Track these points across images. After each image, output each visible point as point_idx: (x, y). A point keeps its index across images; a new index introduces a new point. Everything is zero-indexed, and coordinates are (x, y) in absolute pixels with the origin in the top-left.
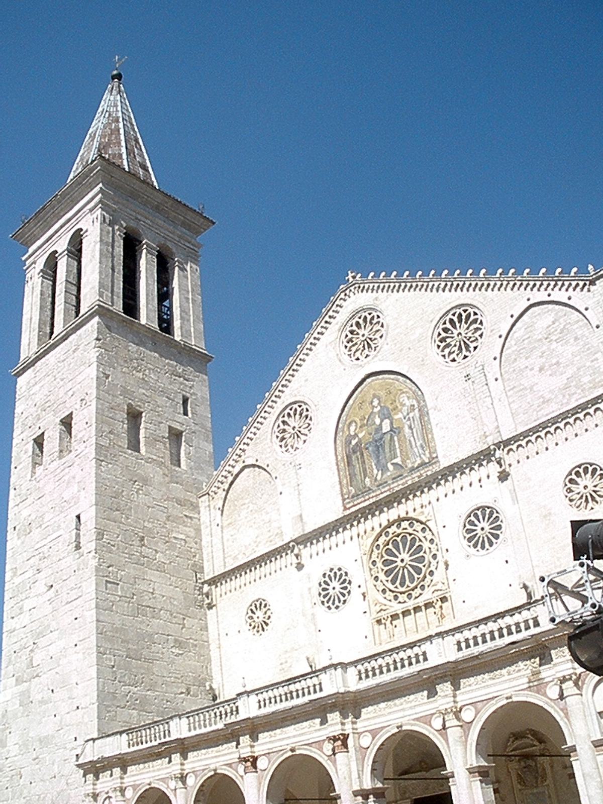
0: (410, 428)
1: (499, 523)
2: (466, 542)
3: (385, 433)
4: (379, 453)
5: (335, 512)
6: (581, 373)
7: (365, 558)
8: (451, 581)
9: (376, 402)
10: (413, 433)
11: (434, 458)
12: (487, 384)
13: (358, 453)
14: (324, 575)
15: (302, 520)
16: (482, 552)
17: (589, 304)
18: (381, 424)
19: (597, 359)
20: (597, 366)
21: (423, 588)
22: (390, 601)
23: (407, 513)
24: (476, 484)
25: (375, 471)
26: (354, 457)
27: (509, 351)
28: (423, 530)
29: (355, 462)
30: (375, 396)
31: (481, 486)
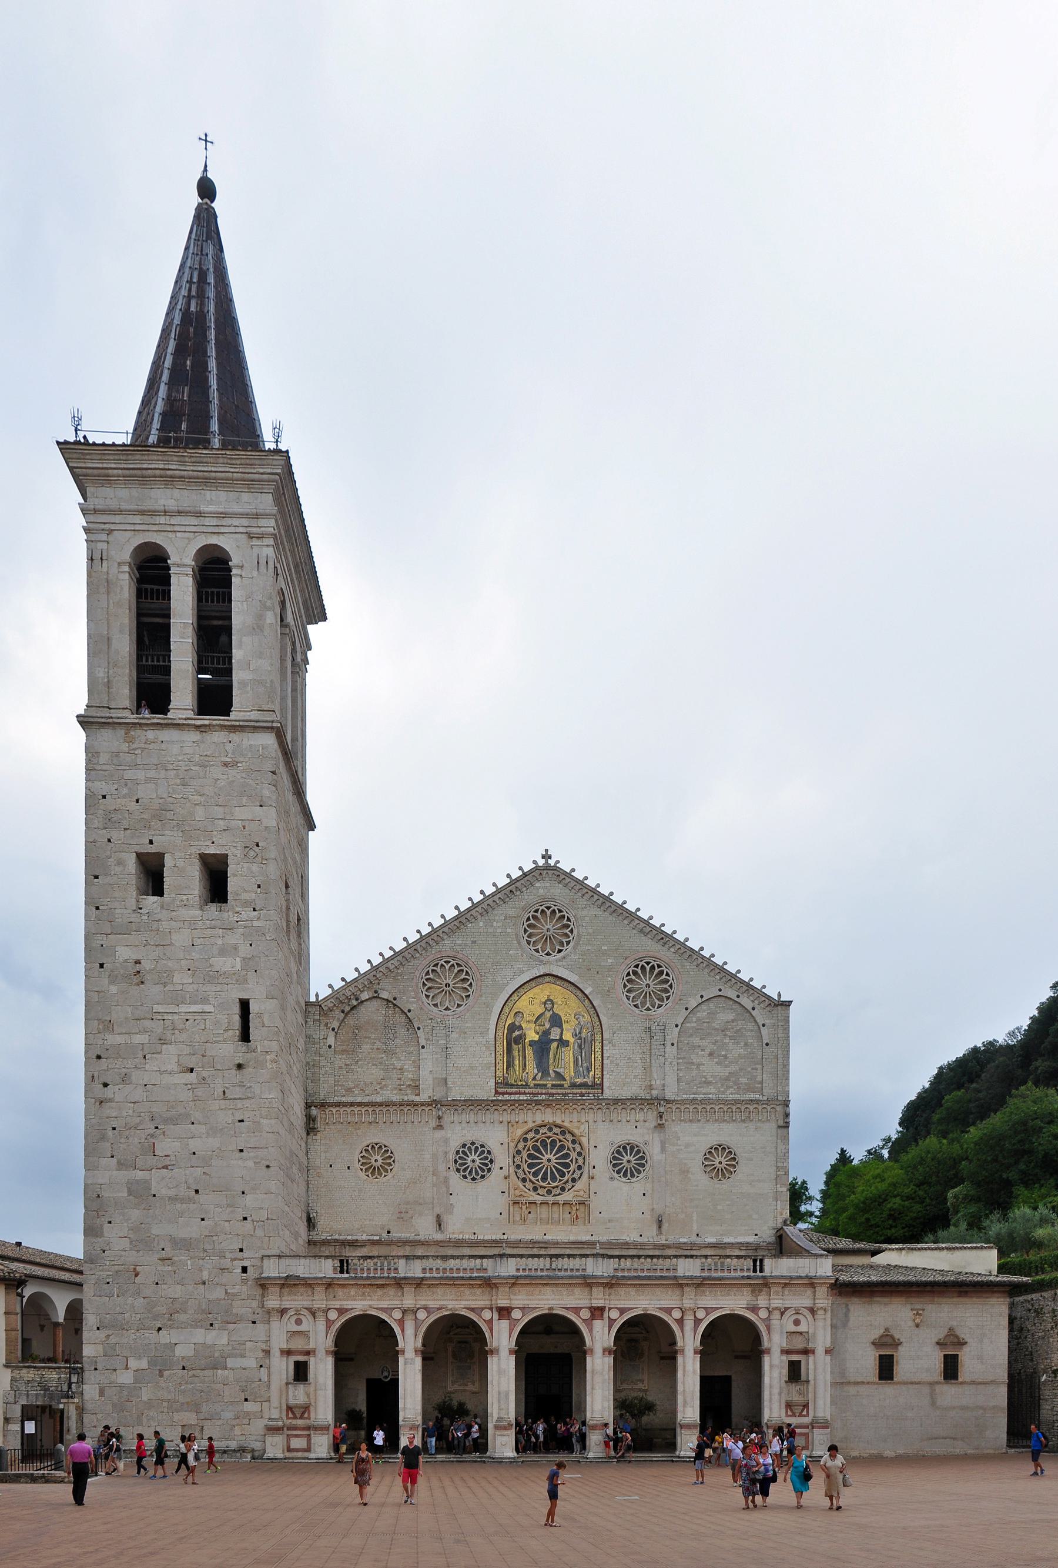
0: (580, 1046)
1: (643, 1162)
2: (611, 1167)
3: (553, 1040)
4: (543, 1055)
5: (486, 1090)
6: (742, 1074)
7: (512, 1145)
8: (592, 1194)
9: (549, 1006)
11: (597, 1084)
12: (664, 1044)
14: (464, 1146)
15: (446, 1084)
16: (624, 1180)
17: (767, 1022)
18: (550, 1029)
19: (756, 1069)
20: (755, 1074)
21: (563, 1189)
22: (529, 1190)
23: (563, 1122)
24: (633, 1124)
25: (536, 1071)
26: (515, 1047)
27: (688, 1025)
28: (574, 1142)
29: (515, 1053)
30: (549, 1000)
31: (636, 1127)
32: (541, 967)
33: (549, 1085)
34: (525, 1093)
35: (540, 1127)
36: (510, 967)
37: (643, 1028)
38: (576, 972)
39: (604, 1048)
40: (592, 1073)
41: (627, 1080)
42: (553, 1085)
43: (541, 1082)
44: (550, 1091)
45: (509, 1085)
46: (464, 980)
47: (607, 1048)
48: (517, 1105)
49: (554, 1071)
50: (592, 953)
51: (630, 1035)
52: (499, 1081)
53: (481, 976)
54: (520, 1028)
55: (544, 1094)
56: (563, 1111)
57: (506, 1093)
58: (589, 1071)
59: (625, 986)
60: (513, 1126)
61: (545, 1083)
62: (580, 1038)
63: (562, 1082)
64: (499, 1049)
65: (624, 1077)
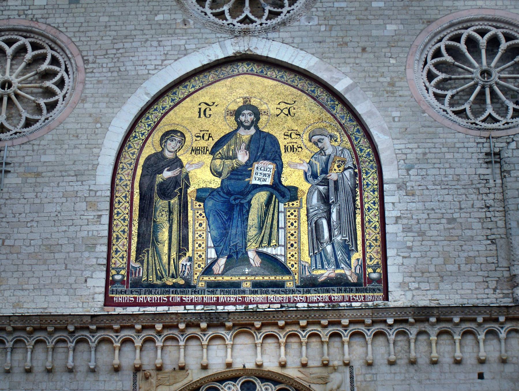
0: (325, 199)
3: (256, 187)
4: (230, 219)
9: (247, 117)
10: (329, 213)
11: (371, 281)
13: (174, 201)
18: (249, 164)
25: (212, 254)
26: (161, 204)
30: (247, 106)
31: (481, 376)
32: (228, 42)
33: (247, 286)
34: (182, 303)
35: (222, 381)
36: (155, 44)
37: (482, 156)
38: (314, 51)
39: (387, 199)
40: (357, 256)
41: (450, 267)
42: (257, 285)
43: (227, 278)
44: (250, 297)
45: (142, 286)
46: (47, 75)
47: (395, 199)
48: (159, 327)
49: (260, 254)
50: (350, 13)
51: (450, 171)
52: (118, 277)
53: (86, 62)
54: (176, 163)
55: (234, 304)
56: (282, 340)
57: (135, 304)
58: (348, 251)
59: (430, 76)
60: (147, 378)
61: (235, 279)
62: (325, 182)
63: (279, 278)
64: (122, 208)
65: (440, 261)
